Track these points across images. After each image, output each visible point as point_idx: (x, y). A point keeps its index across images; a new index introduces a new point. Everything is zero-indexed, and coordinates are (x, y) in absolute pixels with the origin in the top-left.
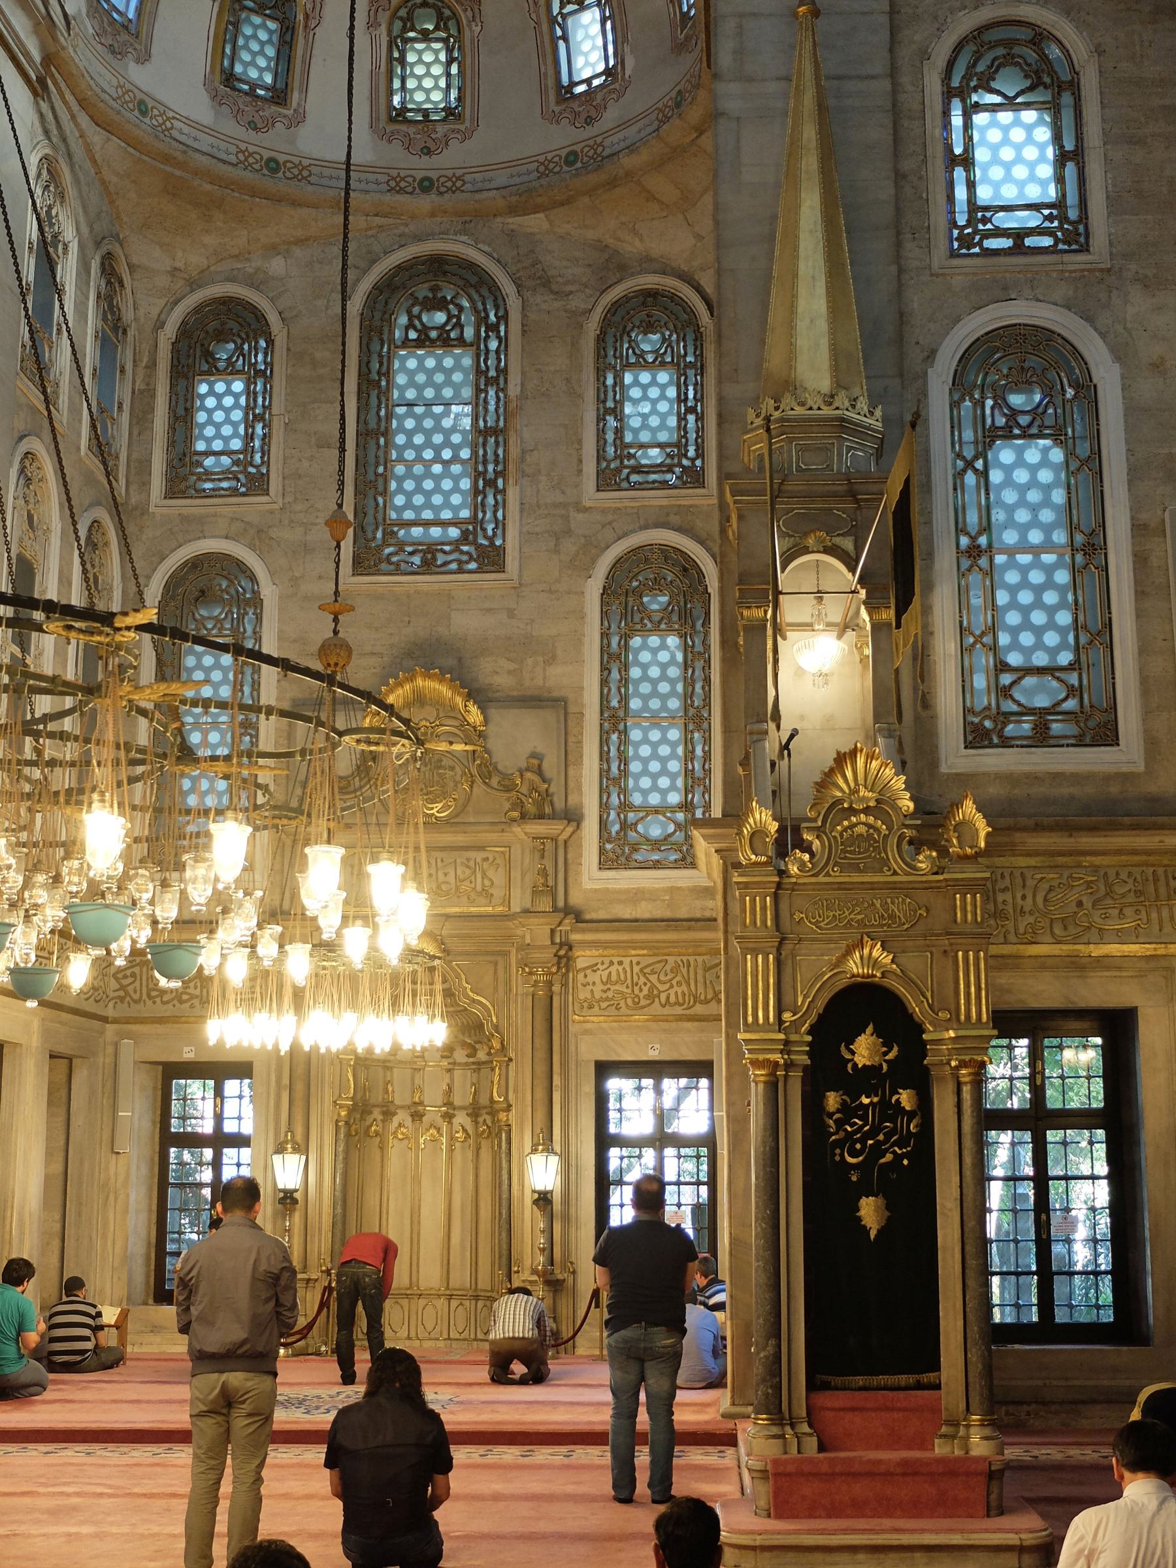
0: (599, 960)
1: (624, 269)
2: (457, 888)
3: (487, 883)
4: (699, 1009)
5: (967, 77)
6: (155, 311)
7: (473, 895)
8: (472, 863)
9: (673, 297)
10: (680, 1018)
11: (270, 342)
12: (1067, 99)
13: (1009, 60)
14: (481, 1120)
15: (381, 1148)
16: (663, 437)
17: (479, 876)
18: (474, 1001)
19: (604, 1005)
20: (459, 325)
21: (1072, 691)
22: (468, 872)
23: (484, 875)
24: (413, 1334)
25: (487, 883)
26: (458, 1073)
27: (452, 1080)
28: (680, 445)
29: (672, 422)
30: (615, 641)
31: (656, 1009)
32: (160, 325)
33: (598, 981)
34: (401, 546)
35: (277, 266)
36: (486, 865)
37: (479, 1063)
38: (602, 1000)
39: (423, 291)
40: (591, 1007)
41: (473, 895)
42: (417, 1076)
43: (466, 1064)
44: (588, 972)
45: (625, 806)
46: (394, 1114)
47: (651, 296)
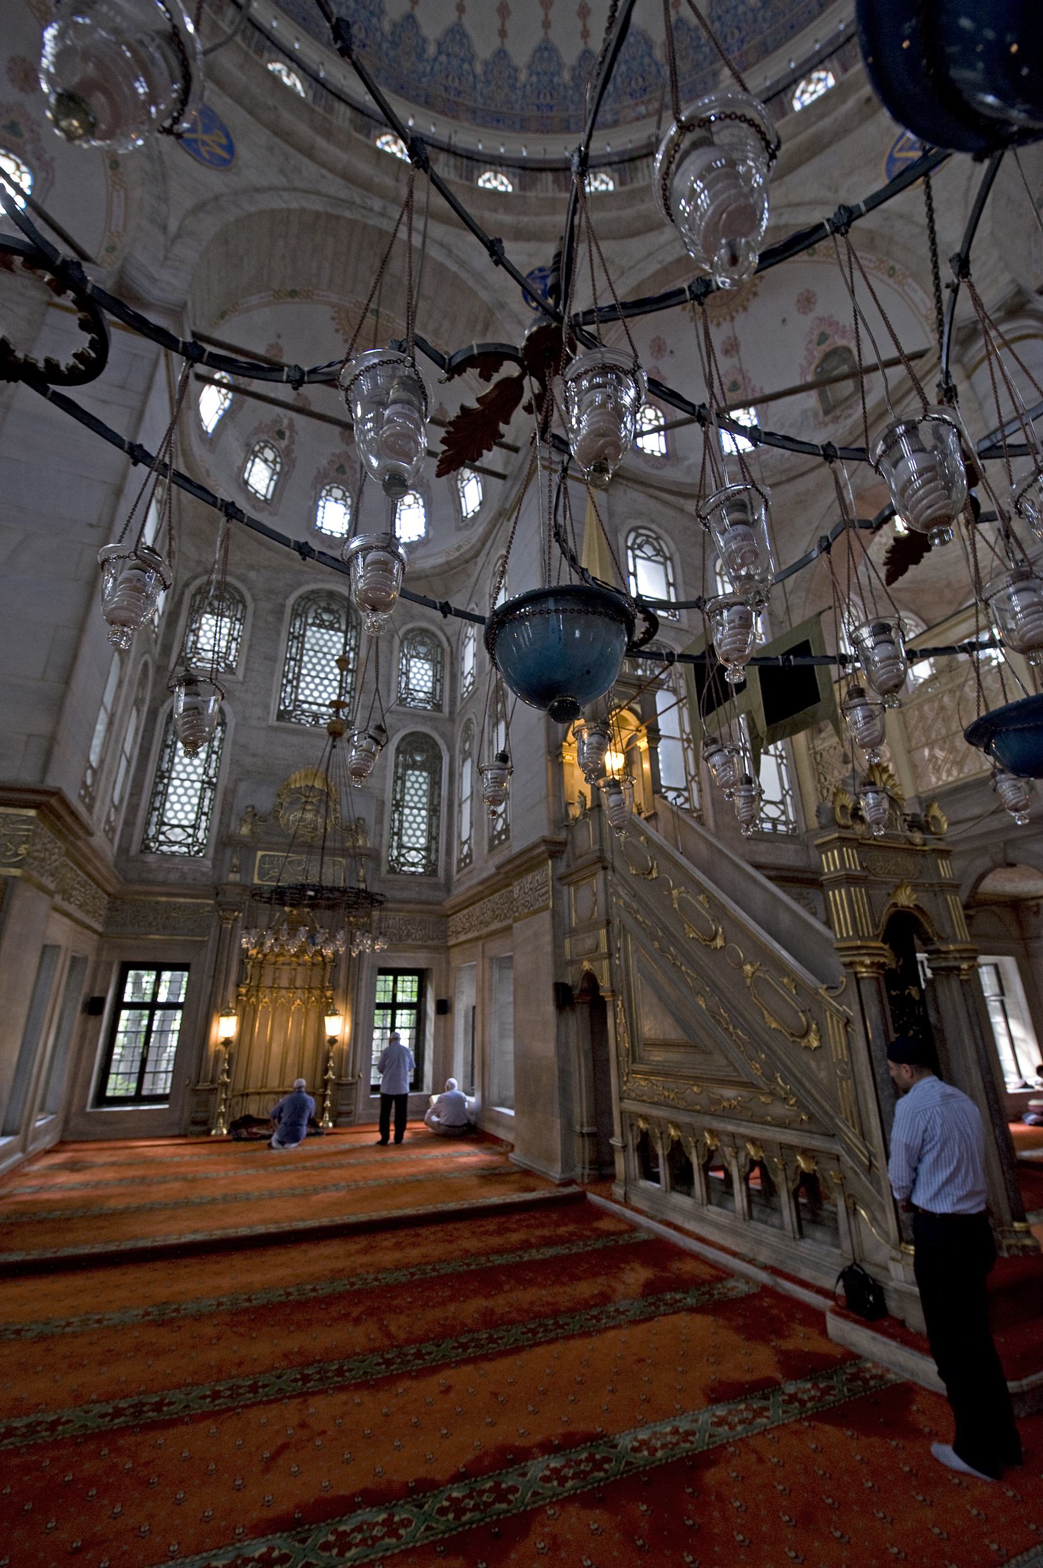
1: (412, 618)
4: (430, 943)
5: (634, 543)
6: (185, 578)
9: (433, 634)
10: (421, 947)
11: (245, 607)
12: (669, 563)
13: (647, 542)
16: (425, 689)
20: (338, 622)
21: (687, 800)
28: (433, 693)
29: (430, 684)
30: (400, 770)
31: (410, 941)
32: (187, 585)
34: (303, 712)
35: (252, 575)
39: (323, 604)
45: (401, 846)
47: (423, 631)
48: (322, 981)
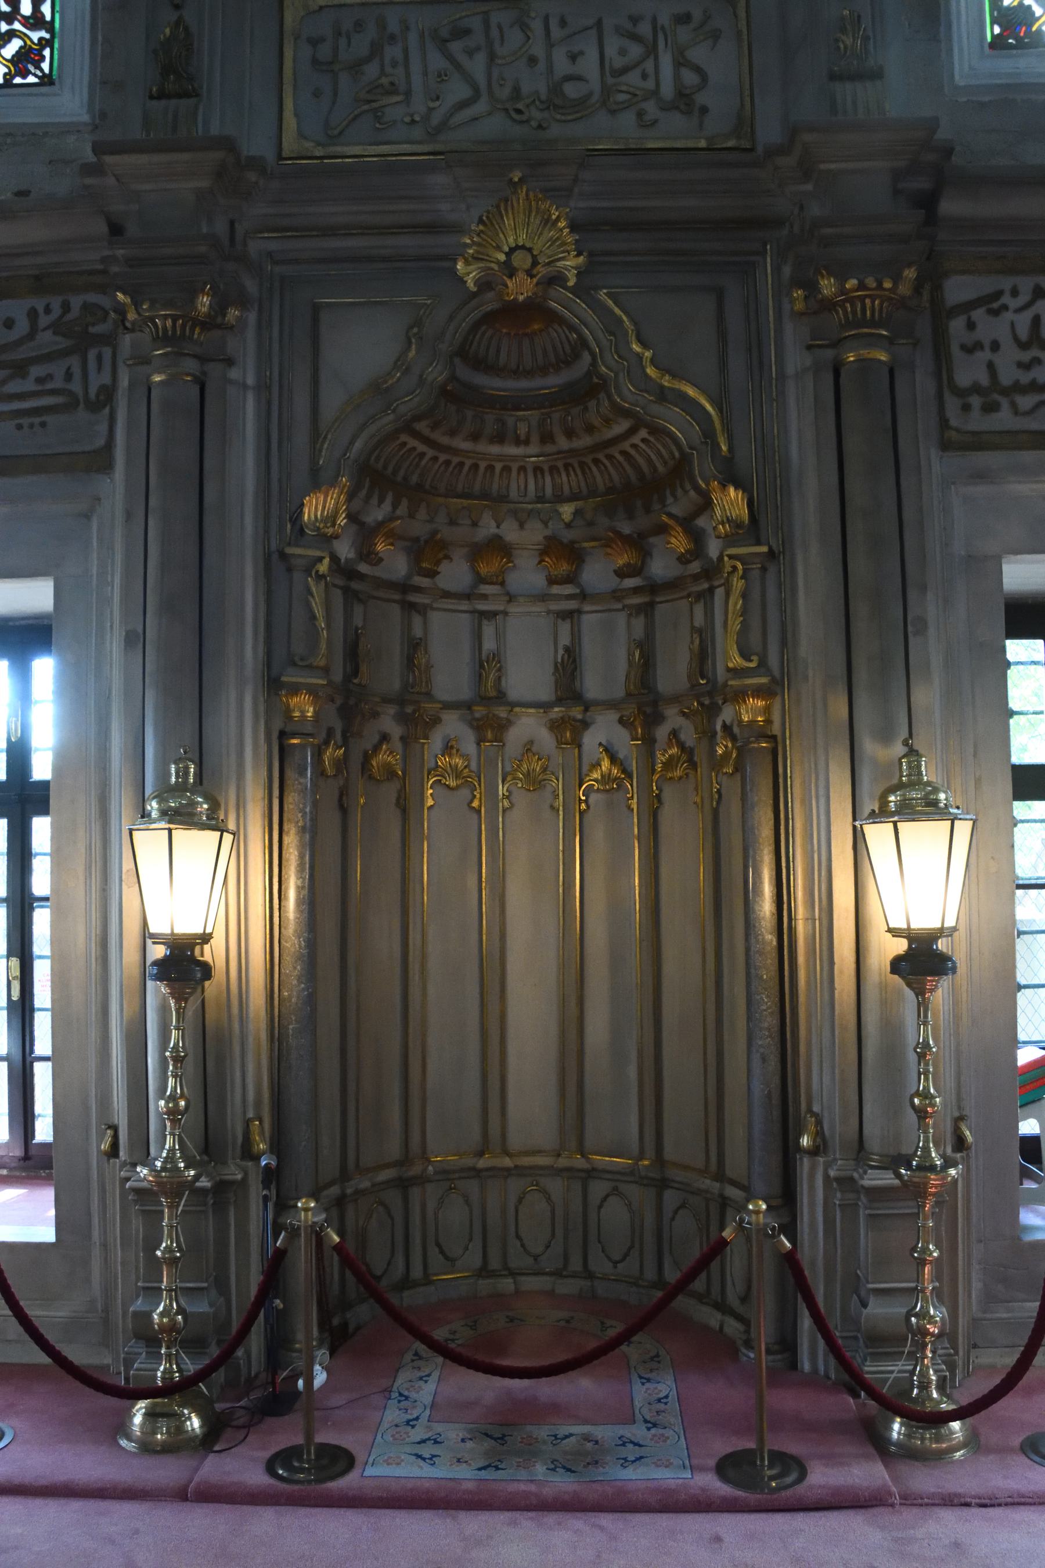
0: (1006, 283)
2: (607, 91)
3: (690, 78)
7: (651, 108)
8: (644, 29)
14: (662, 733)
15: (404, 811)
17: (666, 62)
18: (663, 395)
19: (1026, 402)
22: (636, 50)
23: (680, 62)
24: (495, 1264)
25: (690, 78)
26: (590, 621)
27: (576, 635)
33: (1003, 335)
36: (684, 34)
37: (653, 588)
38: (1018, 388)
40: (990, 408)
41: (651, 108)
42: (488, 630)
43: (617, 595)
44: (978, 314)
46: (436, 721)
48: (703, 656)
